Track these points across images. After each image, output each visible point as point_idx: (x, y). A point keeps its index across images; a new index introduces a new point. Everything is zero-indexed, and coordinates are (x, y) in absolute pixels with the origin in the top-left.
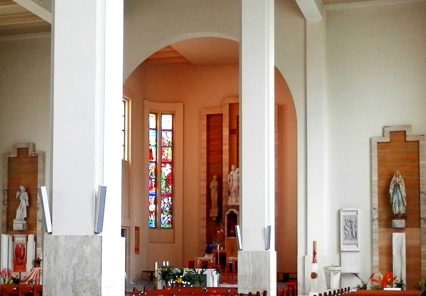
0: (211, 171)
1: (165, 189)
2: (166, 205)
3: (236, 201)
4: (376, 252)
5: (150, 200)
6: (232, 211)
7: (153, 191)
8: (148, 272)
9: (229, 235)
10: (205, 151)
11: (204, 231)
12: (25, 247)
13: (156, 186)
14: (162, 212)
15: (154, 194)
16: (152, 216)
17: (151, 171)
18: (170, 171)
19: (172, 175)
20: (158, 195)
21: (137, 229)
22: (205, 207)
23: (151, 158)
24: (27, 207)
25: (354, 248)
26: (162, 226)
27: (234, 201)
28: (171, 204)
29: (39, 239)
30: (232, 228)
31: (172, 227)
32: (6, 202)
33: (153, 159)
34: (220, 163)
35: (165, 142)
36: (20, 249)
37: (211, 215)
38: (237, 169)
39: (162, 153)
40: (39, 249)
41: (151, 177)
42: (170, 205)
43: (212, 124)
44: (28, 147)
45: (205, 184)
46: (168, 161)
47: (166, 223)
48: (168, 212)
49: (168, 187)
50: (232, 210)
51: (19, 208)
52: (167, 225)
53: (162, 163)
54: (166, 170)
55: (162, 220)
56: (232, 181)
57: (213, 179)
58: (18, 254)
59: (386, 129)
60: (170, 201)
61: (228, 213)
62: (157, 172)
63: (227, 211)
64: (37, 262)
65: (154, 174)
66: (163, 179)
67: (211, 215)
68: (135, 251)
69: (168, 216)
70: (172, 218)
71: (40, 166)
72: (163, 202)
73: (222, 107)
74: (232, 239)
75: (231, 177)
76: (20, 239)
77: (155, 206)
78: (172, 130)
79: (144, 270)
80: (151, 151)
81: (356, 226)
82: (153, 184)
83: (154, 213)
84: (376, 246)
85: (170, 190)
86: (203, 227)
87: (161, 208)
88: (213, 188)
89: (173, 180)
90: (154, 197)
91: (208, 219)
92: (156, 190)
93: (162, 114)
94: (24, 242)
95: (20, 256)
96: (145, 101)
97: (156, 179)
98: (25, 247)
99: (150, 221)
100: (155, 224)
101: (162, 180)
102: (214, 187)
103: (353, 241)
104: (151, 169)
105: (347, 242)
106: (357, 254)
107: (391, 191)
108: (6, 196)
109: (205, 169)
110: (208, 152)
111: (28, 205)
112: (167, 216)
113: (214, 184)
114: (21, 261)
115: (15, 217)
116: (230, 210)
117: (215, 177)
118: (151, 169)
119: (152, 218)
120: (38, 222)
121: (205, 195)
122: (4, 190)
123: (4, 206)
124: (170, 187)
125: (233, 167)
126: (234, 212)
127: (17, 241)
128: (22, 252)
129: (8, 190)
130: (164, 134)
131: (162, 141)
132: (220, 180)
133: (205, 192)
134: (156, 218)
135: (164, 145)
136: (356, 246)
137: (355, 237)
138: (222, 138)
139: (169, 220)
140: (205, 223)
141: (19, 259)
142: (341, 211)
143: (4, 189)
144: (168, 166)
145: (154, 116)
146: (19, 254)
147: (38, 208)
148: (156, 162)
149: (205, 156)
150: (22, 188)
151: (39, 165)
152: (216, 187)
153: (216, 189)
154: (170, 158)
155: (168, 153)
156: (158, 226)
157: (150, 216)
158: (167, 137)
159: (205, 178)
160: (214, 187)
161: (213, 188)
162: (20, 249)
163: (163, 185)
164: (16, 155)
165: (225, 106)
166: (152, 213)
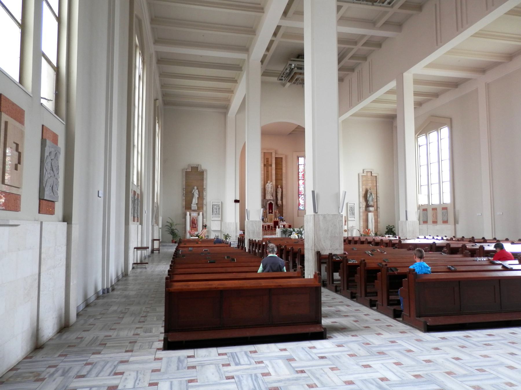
4: (362, 221)
6: (271, 202)
9: (269, 213)
24: (198, 197)
25: (353, 219)
27: (270, 197)
32: (185, 195)
38: (271, 183)
50: (271, 201)
51: (194, 198)
59: (365, 170)
61: (269, 202)
64: (205, 227)
71: (205, 176)
76: (194, 214)
81: (354, 210)
84: (361, 218)
95: (195, 223)
103: (353, 216)
105: (351, 216)
106: (354, 221)
107: (368, 196)
108: (185, 191)
115: (192, 204)
122: (184, 188)
129: (186, 188)
136: (354, 218)
137: (353, 214)
142: (348, 204)
146: (194, 222)
150: (196, 188)
151: (204, 176)
162: (195, 220)
164: (190, 170)
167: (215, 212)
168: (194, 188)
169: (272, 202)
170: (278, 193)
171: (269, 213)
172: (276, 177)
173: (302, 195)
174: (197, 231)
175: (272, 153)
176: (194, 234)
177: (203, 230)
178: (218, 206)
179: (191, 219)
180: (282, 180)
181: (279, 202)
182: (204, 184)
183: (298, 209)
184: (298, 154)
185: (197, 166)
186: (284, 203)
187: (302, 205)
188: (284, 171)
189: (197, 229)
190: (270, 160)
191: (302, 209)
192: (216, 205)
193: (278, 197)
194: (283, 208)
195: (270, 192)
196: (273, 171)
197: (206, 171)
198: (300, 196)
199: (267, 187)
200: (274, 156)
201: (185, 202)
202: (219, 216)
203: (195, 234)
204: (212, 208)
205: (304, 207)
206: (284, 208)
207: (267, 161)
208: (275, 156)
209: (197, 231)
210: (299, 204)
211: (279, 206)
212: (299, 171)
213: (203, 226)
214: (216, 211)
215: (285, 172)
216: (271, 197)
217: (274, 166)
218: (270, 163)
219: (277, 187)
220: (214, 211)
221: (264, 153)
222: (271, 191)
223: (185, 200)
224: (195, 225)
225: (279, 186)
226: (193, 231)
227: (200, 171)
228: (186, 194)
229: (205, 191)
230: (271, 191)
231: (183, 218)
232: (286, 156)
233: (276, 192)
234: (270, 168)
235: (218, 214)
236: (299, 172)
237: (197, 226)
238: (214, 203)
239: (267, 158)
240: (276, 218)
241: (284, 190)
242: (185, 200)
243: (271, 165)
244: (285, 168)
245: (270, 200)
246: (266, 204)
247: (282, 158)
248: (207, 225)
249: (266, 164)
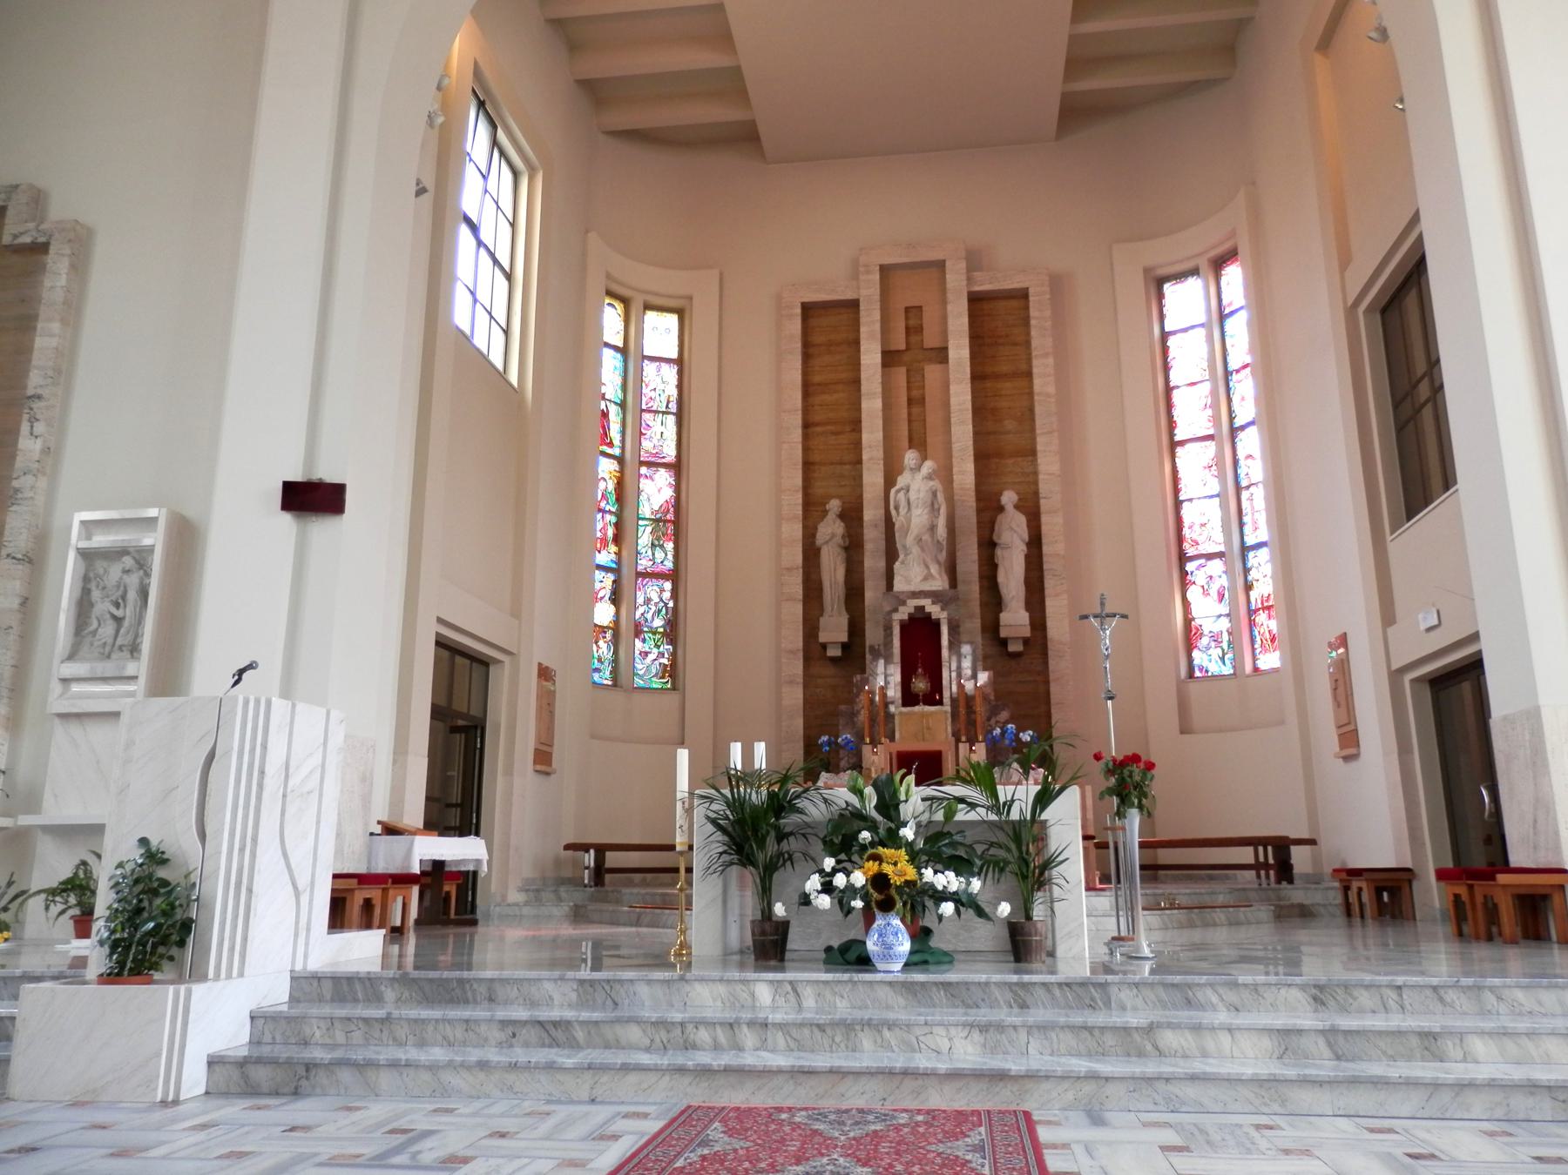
0: (819, 489)
1: (650, 553)
2: (653, 608)
3: (925, 579)
5: (598, 586)
6: (921, 609)
7: (605, 557)
8: (585, 848)
10: (797, 420)
11: (795, 696)
13: (617, 539)
14: (638, 631)
15: (614, 566)
16: (601, 643)
17: (602, 485)
18: (669, 493)
19: (677, 503)
20: (625, 571)
21: (545, 673)
22: (798, 609)
23: (605, 438)
26: (639, 682)
28: (671, 604)
30: (920, 670)
31: (674, 688)
33: (611, 445)
34: (850, 463)
35: (652, 394)
37: (823, 637)
39: (643, 431)
41: (603, 504)
42: (667, 608)
43: (818, 338)
44: (9, 199)
45: (795, 530)
46: (664, 461)
47: (654, 671)
48: (660, 633)
49: (662, 547)
52: (654, 679)
53: (642, 463)
54: (656, 491)
55: (637, 660)
56: (906, 510)
57: (825, 512)
60: (667, 595)
61: (903, 614)
62: (623, 492)
63: (901, 609)
65: (613, 498)
66: (647, 517)
67: (823, 638)
68: (535, 762)
69: (661, 649)
70: (674, 655)
72: (640, 600)
73: (855, 276)
74: (923, 715)
75: (901, 495)
77: (612, 609)
78: (679, 362)
79: (572, 840)
80: (605, 415)
82: (610, 532)
83: (609, 635)
85: (670, 557)
86: (791, 682)
87: (637, 617)
88: (827, 542)
89: (676, 523)
90: (611, 577)
91: (813, 649)
92: (618, 554)
93: (648, 307)
96: (592, 236)
97: (619, 515)
99: (596, 661)
100: (615, 672)
101: (640, 522)
102: (830, 540)
104: (605, 480)
109: (799, 481)
110: (806, 425)
112: (658, 647)
113: (831, 530)
116: (913, 603)
117: (834, 505)
118: (605, 480)
119: (604, 649)
121: (797, 568)
124: (670, 546)
125: (910, 457)
126: (928, 609)
130: (649, 369)
131: (644, 391)
132: (852, 516)
133: (799, 559)
134: (616, 652)
135: (649, 405)
138: (856, 382)
139: (665, 661)
140: (797, 667)
144: (664, 478)
145: (620, 307)
147: (17, 491)
148: (620, 460)
149: (797, 434)
152: (838, 540)
153: (840, 546)
154: (670, 452)
155: (661, 437)
156: (623, 679)
157: (596, 643)
158: (661, 383)
159: (799, 511)
160: (830, 540)
161: (827, 542)
163: (645, 538)
165: (868, 272)
166: (605, 632)
167: (108, 629)
169: (934, 610)
170: (999, 552)
171: (909, 698)
172: (978, 434)
173: (1210, 557)
175: (940, 265)
178: (141, 559)
180: (1032, 453)
181: (1015, 618)
183: (1183, 672)
184: (1160, 253)
186: (1058, 626)
187: (1216, 638)
188: (1043, 383)
190: (929, 319)
191: (1215, 668)
193: (1001, 578)
194: (1052, 663)
195: (919, 540)
196: (953, 389)
197: (81, 240)
198: (1190, 567)
199: (903, 503)
200: (956, 281)
202: (131, 668)
205: (1229, 656)
206: (1060, 665)
207: (913, 330)
208: (969, 279)
210: (1191, 635)
211: (1012, 648)
212: (1175, 378)
214: (115, 618)
215: (1051, 389)
216: (927, 578)
217: (960, 352)
218: (930, 339)
219: (989, 508)
221: (884, 269)
222: (932, 528)
225: (1009, 498)
227: (15, 236)
229: (33, 420)
230: (932, 528)
232: (1058, 284)
233: (988, 546)
234: (932, 372)
236: (1169, 390)
238: (101, 540)
239: (907, 310)
240: (972, 741)
241: (1051, 525)
243: (941, 355)
244: (1051, 361)
245: (915, 595)
246: (888, 629)
247: (1023, 295)
249: (899, 343)
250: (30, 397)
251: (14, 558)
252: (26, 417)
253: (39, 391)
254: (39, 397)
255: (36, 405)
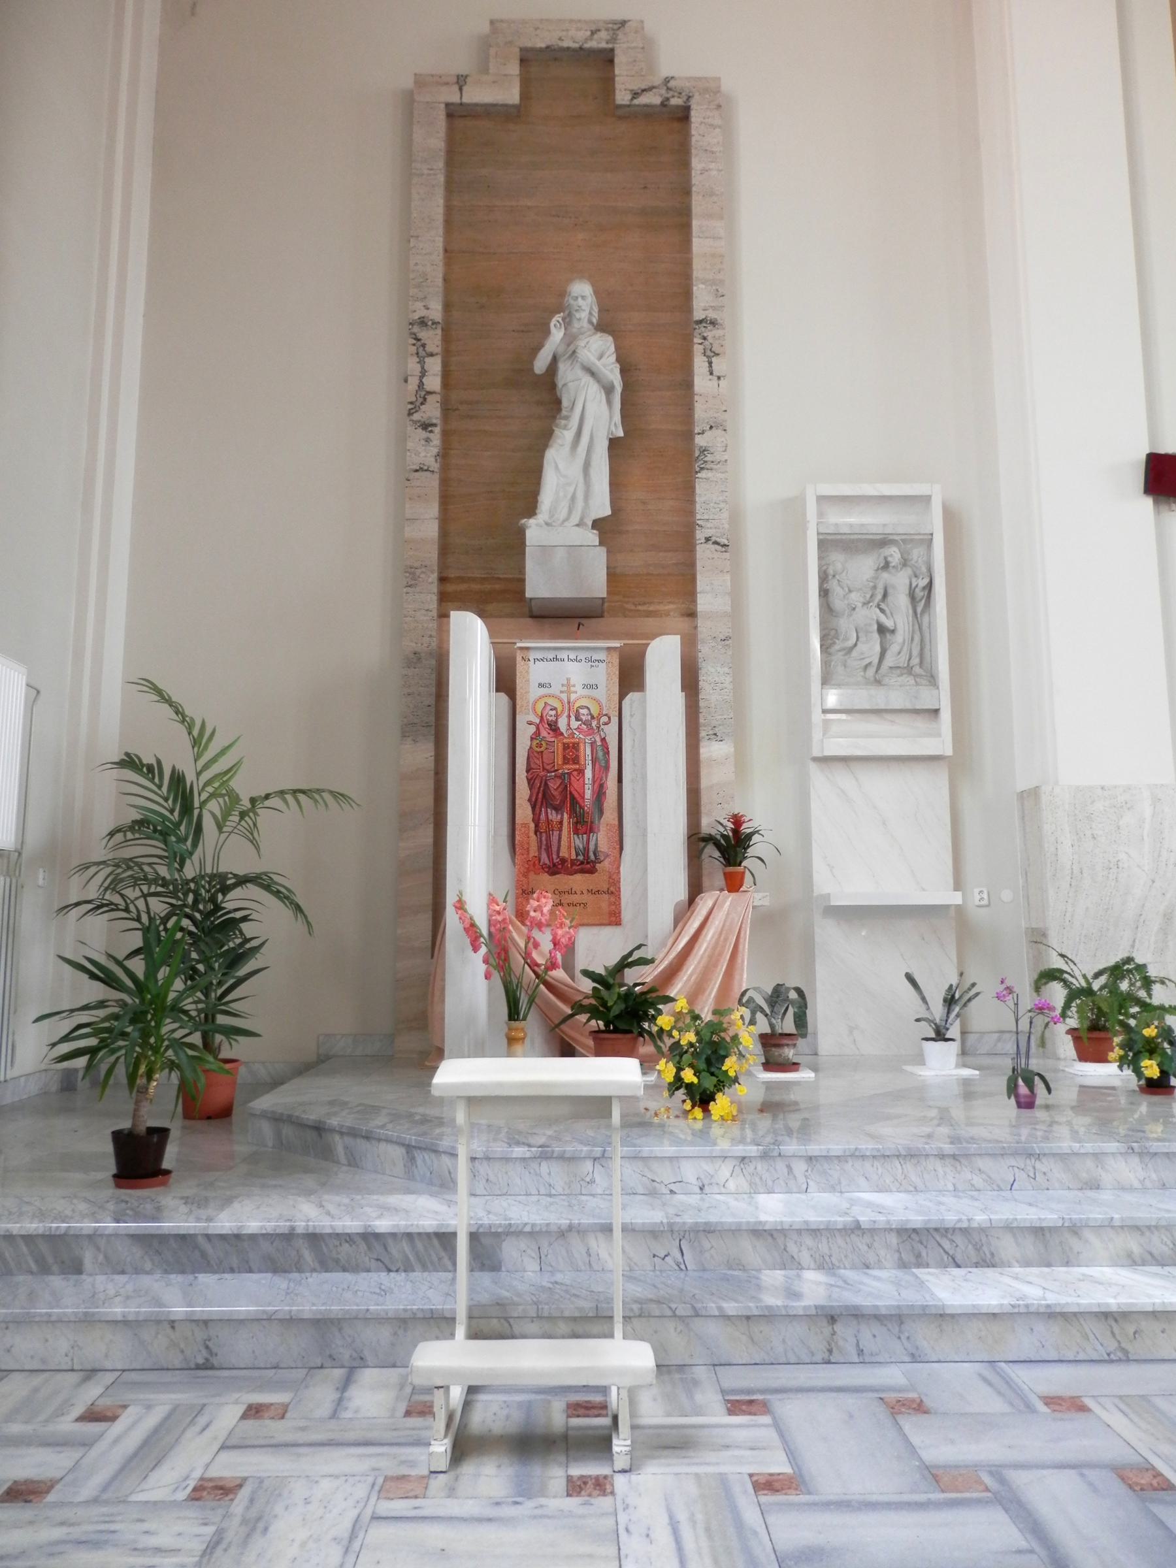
12: (611, 731)
24: (614, 443)
29: (712, 675)
32: (432, 410)
36: (566, 747)
40: (710, 750)
44: (614, 39)
51: (564, 435)
58: (553, 785)
94: (601, 694)
95: (571, 802)
98: (611, 731)
108: (435, 366)
111: (621, 433)
114: (579, 842)
115: (531, 509)
120: (704, 553)
122: (423, 322)
123: (424, 434)
127: (541, 685)
128: (588, 773)
141: (561, 823)
143: (416, 316)
147: (704, 451)
150: (583, 295)
162: (571, 752)
164: (511, 95)
167: (871, 647)
168: (559, 305)
174: (614, 918)
176: (569, 949)
177: (705, 903)
179: (525, 733)
182: (699, 269)
185: (599, 42)
189: (613, 890)
192: (883, 542)
201: (434, 510)
202: (926, 700)
203: (581, 963)
204: (824, 593)
209: (614, 918)
213: (697, 841)
214: (882, 630)
220: (845, 625)
223: (445, 482)
224: (584, 824)
226: (543, 905)
227: (636, 95)
228: (447, 410)
229: (711, 355)
231: (409, 730)
235: (909, 670)
237: (602, 839)
242: (431, 484)
248: (746, 829)
250: (701, 322)
251: (716, 543)
252: (698, 349)
253: (712, 315)
254: (713, 323)
255: (710, 333)
